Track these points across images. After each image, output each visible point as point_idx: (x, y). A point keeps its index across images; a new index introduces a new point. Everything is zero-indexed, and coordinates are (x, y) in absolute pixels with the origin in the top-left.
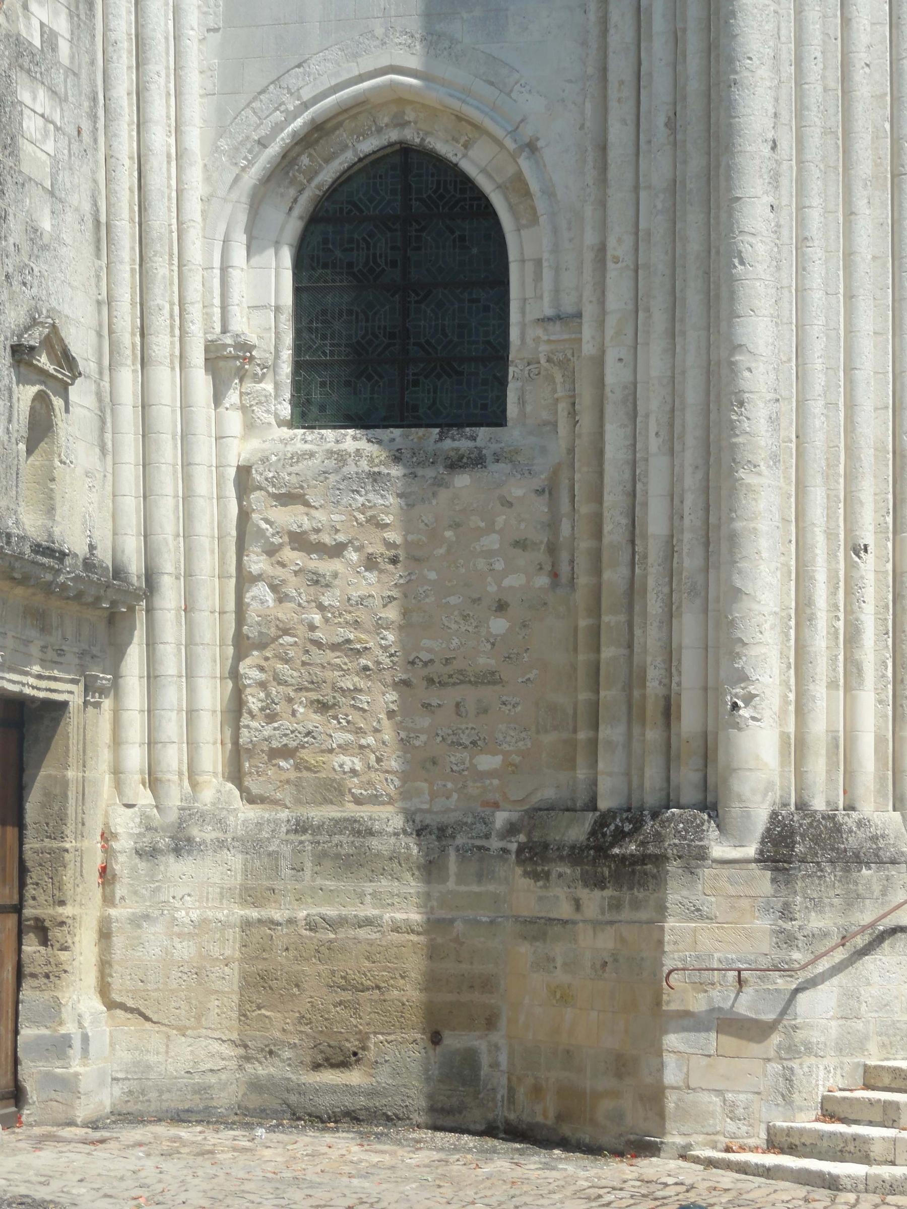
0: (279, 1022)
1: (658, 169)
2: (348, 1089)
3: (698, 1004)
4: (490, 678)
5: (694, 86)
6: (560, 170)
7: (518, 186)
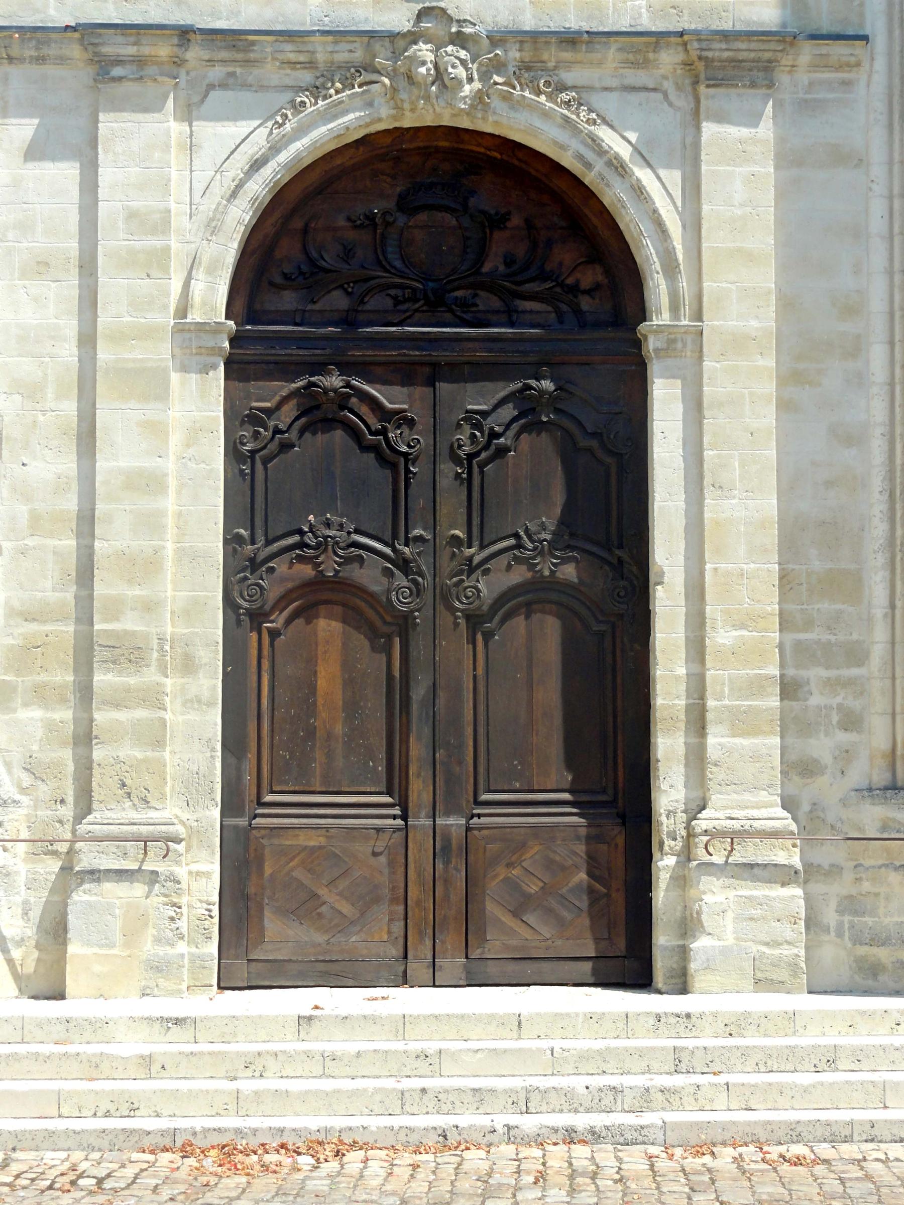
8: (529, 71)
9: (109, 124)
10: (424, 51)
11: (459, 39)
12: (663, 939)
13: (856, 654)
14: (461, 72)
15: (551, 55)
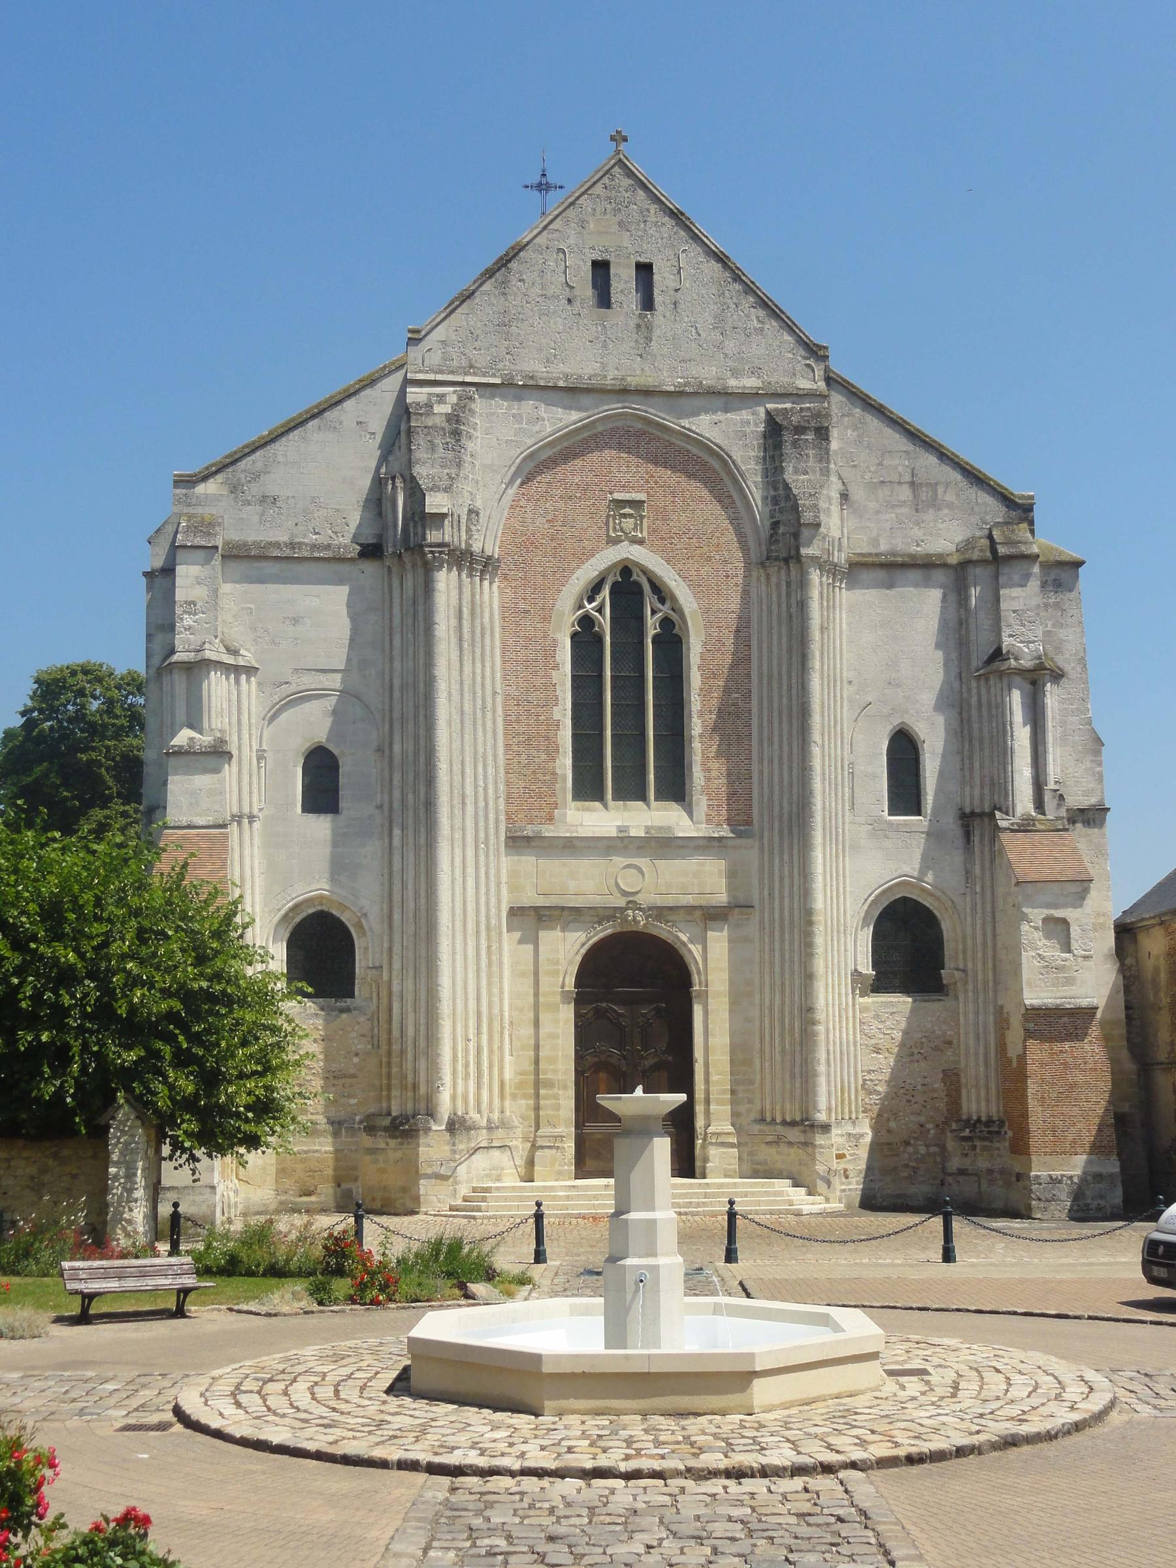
0: (288, 1183)
1: (411, 929)
2: (312, 1202)
3: (429, 1171)
4: (354, 1076)
5: (423, 907)
6: (374, 922)
7: (359, 926)
9: (542, 934)
10: (630, 912)
11: (640, 909)
12: (698, 1164)
13: (751, 1082)
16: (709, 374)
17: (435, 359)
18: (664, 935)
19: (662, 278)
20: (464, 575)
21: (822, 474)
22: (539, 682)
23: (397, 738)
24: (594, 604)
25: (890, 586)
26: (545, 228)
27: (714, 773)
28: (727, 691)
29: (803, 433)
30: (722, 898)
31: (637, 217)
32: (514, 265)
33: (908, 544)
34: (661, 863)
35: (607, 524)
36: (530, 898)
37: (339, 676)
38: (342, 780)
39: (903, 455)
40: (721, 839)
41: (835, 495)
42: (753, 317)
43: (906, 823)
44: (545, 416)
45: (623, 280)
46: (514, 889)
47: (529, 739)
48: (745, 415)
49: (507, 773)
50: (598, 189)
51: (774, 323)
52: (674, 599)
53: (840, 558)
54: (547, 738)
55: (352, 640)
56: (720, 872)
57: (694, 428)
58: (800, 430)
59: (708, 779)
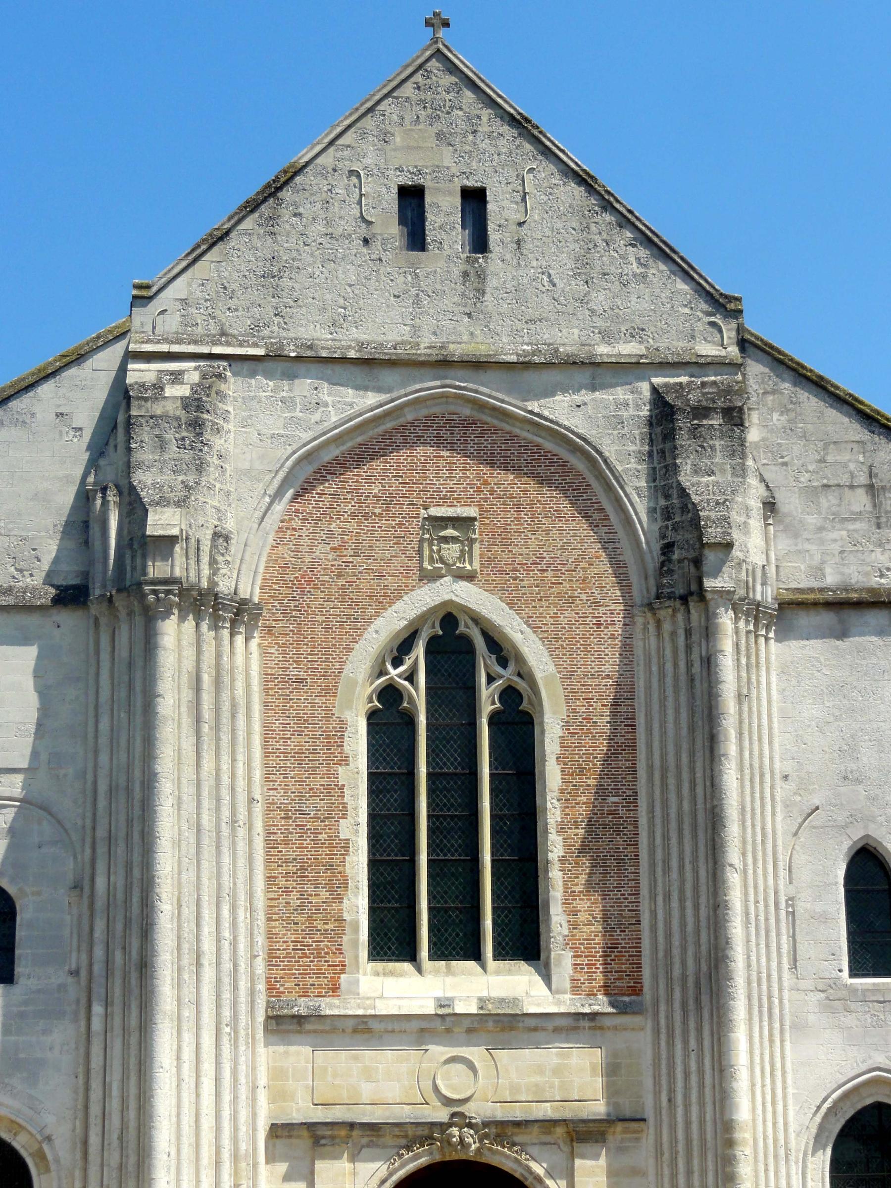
1: (114, 1158)
5: (132, 1124)
6: (62, 1150)
7: (40, 1156)
8: (499, 1138)
9: (319, 1165)
10: (455, 1131)
11: (470, 1126)
14: (471, 1140)
15: (509, 1131)
16: (568, 338)
17: (172, 323)
18: (508, 1166)
19: (500, 208)
20: (204, 626)
21: (734, 474)
22: (318, 782)
23: (101, 867)
24: (401, 669)
25: (842, 634)
26: (331, 143)
27: (583, 917)
28: (601, 792)
29: (706, 417)
30: (598, 1108)
31: (463, 125)
32: (286, 194)
33: (867, 574)
34: (503, 1055)
35: (420, 552)
36: (301, 1110)
37: (19, 779)
38: (20, 933)
39: (855, 446)
40: (593, 1016)
41: (756, 505)
42: (632, 259)
43: (876, 990)
44: (329, 399)
45: (443, 212)
46: (278, 1096)
47: (303, 869)
48: (621, 393)
49: (269, 920)
50: (408, 90)
51: (662, 267)
52: (520, 659)
53: (766, 594)
54: (331, 867)
55: (39, 725)
56: (593, 1068)
57: (546, 413)
58: (701, 412)
59: (574, 926)
